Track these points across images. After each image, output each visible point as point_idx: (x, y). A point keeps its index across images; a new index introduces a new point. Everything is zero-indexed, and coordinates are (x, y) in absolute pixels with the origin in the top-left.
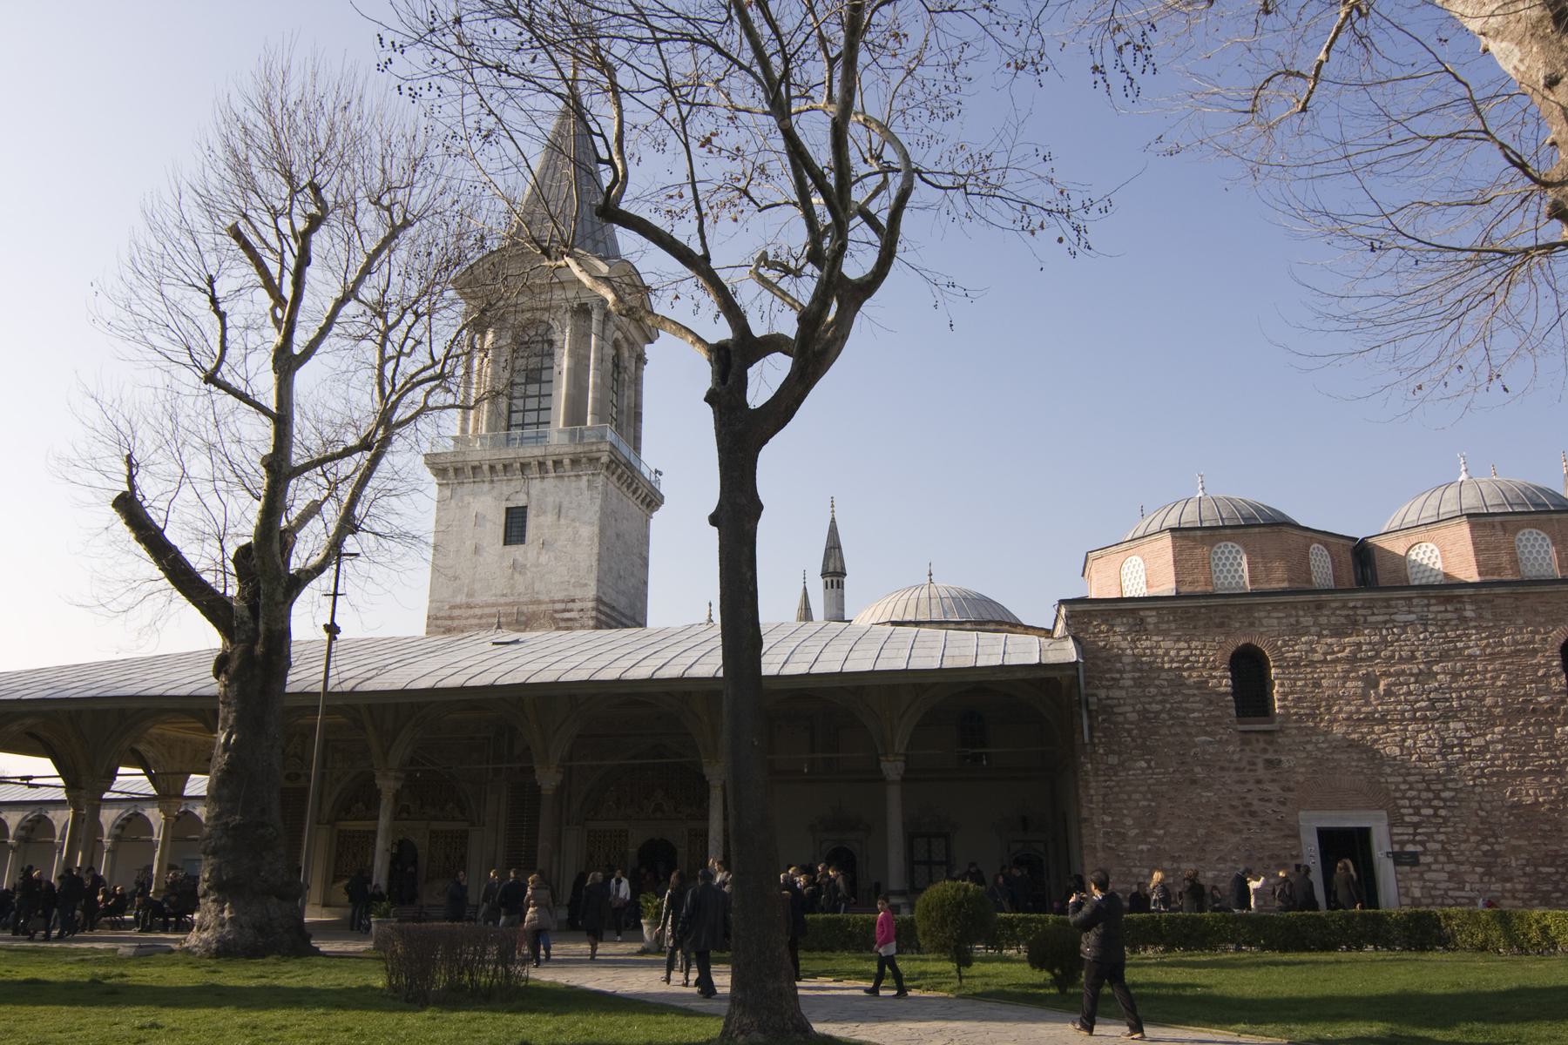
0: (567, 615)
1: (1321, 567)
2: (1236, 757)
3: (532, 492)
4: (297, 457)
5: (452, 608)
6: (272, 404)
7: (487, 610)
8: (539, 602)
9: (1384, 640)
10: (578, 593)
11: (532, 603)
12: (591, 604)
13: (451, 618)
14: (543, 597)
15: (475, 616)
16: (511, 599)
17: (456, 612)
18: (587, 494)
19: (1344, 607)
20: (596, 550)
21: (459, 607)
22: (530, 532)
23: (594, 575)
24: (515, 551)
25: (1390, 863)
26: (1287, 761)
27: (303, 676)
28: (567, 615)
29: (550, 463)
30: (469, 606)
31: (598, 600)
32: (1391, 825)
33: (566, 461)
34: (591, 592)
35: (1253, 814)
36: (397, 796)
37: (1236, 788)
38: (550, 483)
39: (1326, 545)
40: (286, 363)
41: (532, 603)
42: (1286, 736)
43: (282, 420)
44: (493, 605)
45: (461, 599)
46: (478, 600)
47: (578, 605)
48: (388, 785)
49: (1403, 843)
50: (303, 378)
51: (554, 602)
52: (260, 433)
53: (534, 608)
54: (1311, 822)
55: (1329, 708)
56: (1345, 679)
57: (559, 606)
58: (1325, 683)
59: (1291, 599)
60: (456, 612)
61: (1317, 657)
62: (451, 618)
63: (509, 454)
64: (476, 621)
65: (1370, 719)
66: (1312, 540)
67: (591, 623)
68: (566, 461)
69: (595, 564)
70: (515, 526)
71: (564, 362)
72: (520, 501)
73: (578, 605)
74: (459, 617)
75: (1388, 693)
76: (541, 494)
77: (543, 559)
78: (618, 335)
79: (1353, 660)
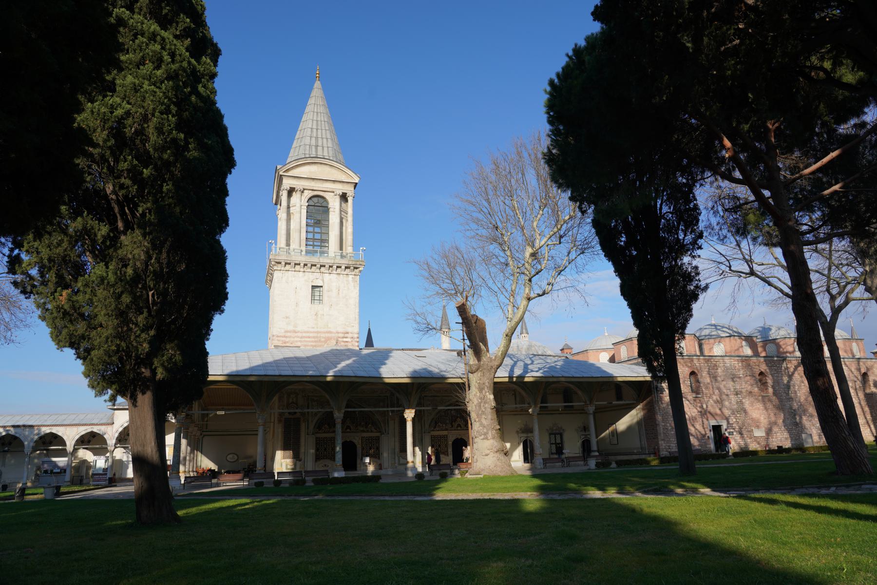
0: (345, 340)
5: (286, 332)
7: (304, 335)
10: (349, 330)
12: (356, 336)
14: (332, 330)
15: (298, 337)
16: (315, 330)
17: (289, 334)
18: (352, 284)
21: (290, 332)
22: (325, 298)
24: (317, 306)
28: (345, 340)
30: (295, 332)
36: (343, 422)
38: (334, 277)
44: (308, 332)
45: (290, 328)
47: (350, 335)
48: (338, 415)
53: (328, 335)
57: (342, 335)
60: (289, 334)
63: (315, 259)
69: (357, 317)
71: (334, 218)
73: (350, 335)
74: (290, 337)
76: (330, 280)
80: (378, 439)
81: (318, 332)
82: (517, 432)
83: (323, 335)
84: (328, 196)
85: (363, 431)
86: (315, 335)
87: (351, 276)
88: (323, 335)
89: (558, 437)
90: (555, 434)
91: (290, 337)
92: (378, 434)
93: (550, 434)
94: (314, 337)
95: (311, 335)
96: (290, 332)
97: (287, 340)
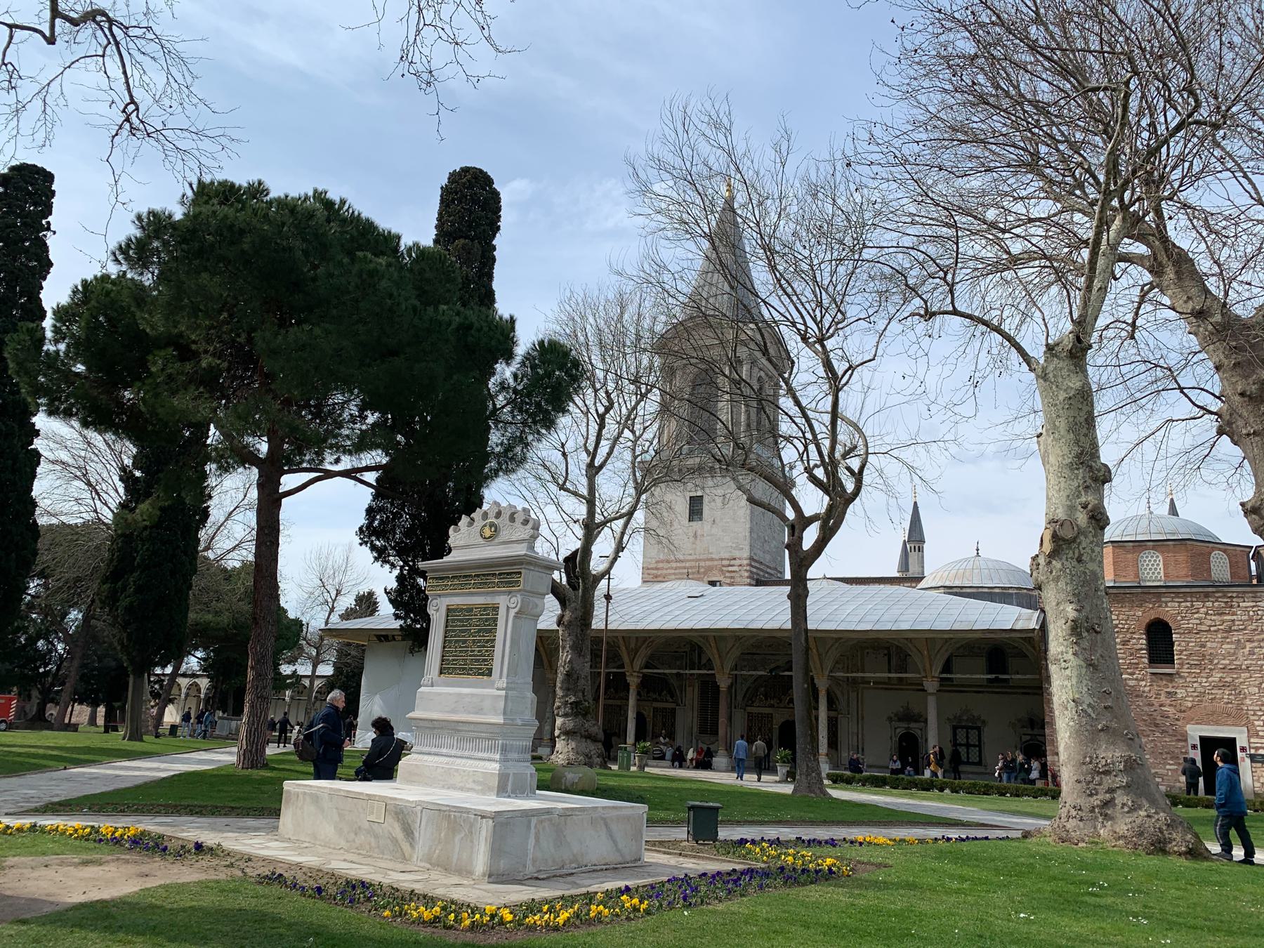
0: (730, 569)
1: (1220, 568)
2: (1147, 689)
4: (599, 518)
6: (584, 492)
8: (712, 559)
9: (1251, 619)
10: (737, 554)
11: (708, 560)
12: (745, 562)
13: (657, 569)
17: (660, 565)
19: (1225, 596)
20: (748, 526)
21: (662, 561)
23: (747, 542)
25: (1248, 760)
26: (1181, 693)
27: (597, 624)
28: (730, 569)
31: (751, 559)
32: (1249, 737)
34: (746, 554)
35: (1157, 725)
37: (1146, 709)
39: (1225, 551)
40: (593, 470)
41: (708, 560)
42: (1181, 677)
43: (591, 503)
47: (737, 562)
49: (1257, 749)
50: (600, 479)
52: (581, 510)
53: (708, 563)
54: (1195, 732)
55: (1211, 661)
56: (1222, 643)
58: (1209, 644)
59: (1188, 590)
60: (660, 565)
61: (1204, 628)
62: (657, 569)
65: (1238, 668)
66: (1213, 549)
67: (747, 574)
69: (748, 534)
74: (662, 569)
75: (1252, 653)
77: (714, 531)
78: (762, 374)
79: (1229, 630)
80: (673, 711)
81: (697, 560)
82: (890, 719)
83: (702, 564)
85: (655, 700)
86: (693, 564)
88: (702, 564)
89: (974, 733)
90: (967, 728)
91: (662, 569)
92: (673, 705)
93: (955, 729)
96: (662, 561)
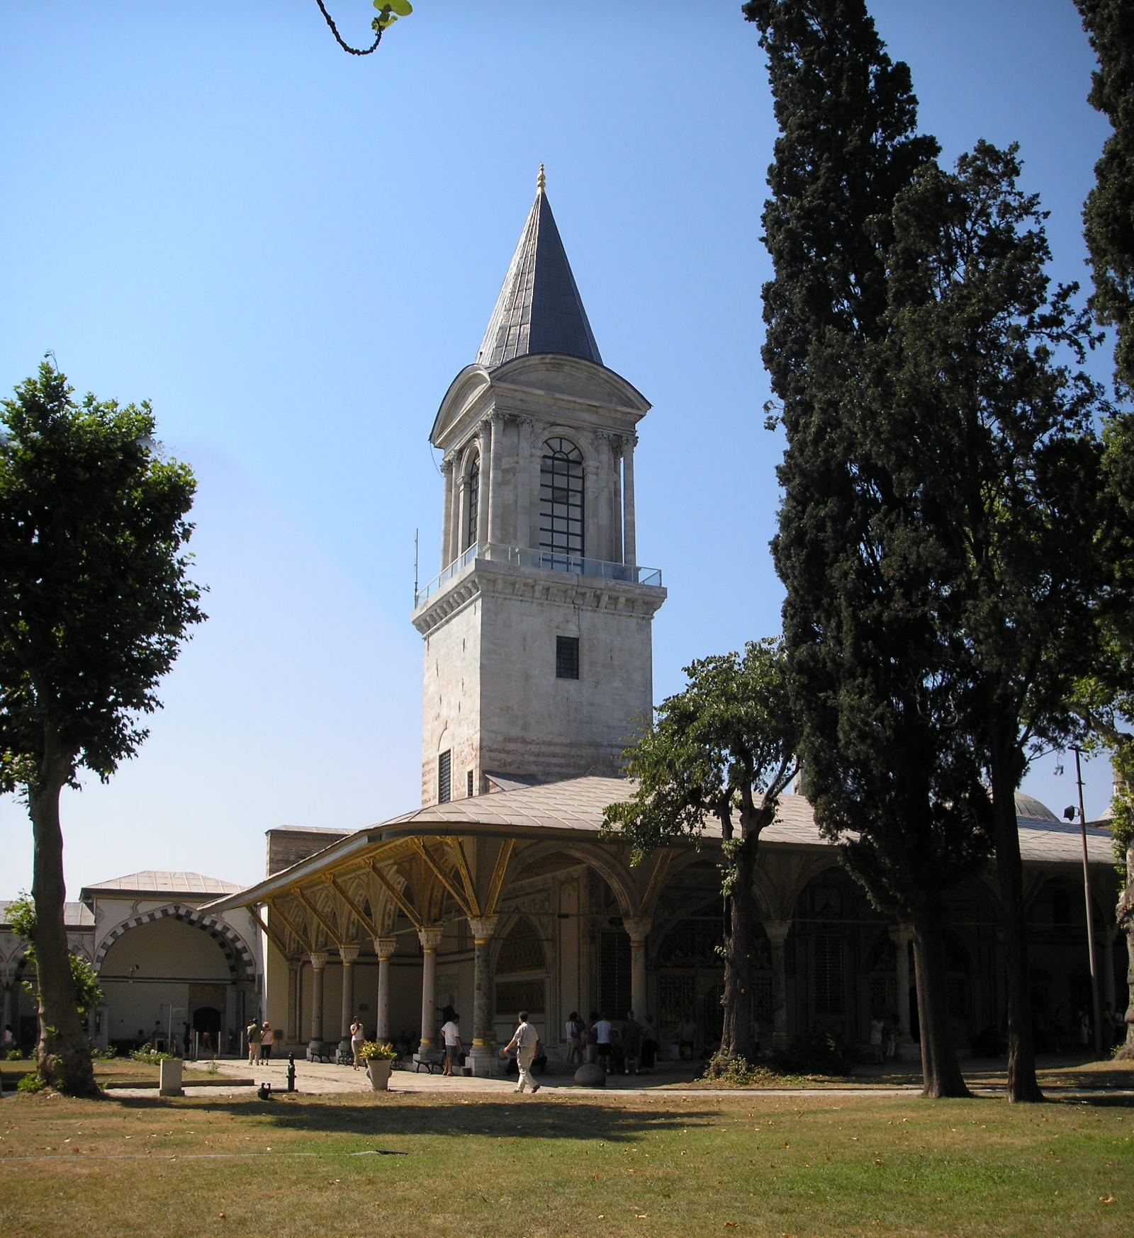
3: (584, 624)
5: (509, 740)
7: (544, 749)
8: (597, 745)
15: (532, 753)
17: (512, 746)
22: (584, 667)
24: (569, 685)
29: (605, 599)
30: (524, 742)
33: (622, 600)
44: (550, 744)
45: (515, 731)
46: (531, 736)
51: (611, 746)
53: (589, 751)
60: (512, 746)
64: (532, 759)
68: (622, 600)
70: (568, 657)
72: (571, 632)
81: (571, 745)
84: (584, 441)
86: (566, 750)
87: (634, 621)
94: (563, 756)
95: (558, 750)
97: (509, 758)
